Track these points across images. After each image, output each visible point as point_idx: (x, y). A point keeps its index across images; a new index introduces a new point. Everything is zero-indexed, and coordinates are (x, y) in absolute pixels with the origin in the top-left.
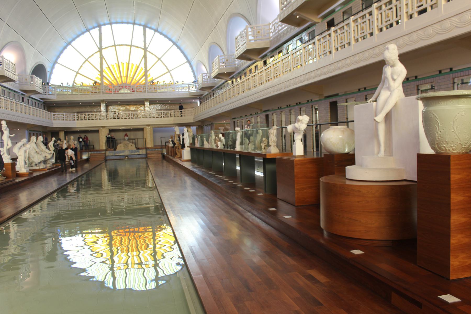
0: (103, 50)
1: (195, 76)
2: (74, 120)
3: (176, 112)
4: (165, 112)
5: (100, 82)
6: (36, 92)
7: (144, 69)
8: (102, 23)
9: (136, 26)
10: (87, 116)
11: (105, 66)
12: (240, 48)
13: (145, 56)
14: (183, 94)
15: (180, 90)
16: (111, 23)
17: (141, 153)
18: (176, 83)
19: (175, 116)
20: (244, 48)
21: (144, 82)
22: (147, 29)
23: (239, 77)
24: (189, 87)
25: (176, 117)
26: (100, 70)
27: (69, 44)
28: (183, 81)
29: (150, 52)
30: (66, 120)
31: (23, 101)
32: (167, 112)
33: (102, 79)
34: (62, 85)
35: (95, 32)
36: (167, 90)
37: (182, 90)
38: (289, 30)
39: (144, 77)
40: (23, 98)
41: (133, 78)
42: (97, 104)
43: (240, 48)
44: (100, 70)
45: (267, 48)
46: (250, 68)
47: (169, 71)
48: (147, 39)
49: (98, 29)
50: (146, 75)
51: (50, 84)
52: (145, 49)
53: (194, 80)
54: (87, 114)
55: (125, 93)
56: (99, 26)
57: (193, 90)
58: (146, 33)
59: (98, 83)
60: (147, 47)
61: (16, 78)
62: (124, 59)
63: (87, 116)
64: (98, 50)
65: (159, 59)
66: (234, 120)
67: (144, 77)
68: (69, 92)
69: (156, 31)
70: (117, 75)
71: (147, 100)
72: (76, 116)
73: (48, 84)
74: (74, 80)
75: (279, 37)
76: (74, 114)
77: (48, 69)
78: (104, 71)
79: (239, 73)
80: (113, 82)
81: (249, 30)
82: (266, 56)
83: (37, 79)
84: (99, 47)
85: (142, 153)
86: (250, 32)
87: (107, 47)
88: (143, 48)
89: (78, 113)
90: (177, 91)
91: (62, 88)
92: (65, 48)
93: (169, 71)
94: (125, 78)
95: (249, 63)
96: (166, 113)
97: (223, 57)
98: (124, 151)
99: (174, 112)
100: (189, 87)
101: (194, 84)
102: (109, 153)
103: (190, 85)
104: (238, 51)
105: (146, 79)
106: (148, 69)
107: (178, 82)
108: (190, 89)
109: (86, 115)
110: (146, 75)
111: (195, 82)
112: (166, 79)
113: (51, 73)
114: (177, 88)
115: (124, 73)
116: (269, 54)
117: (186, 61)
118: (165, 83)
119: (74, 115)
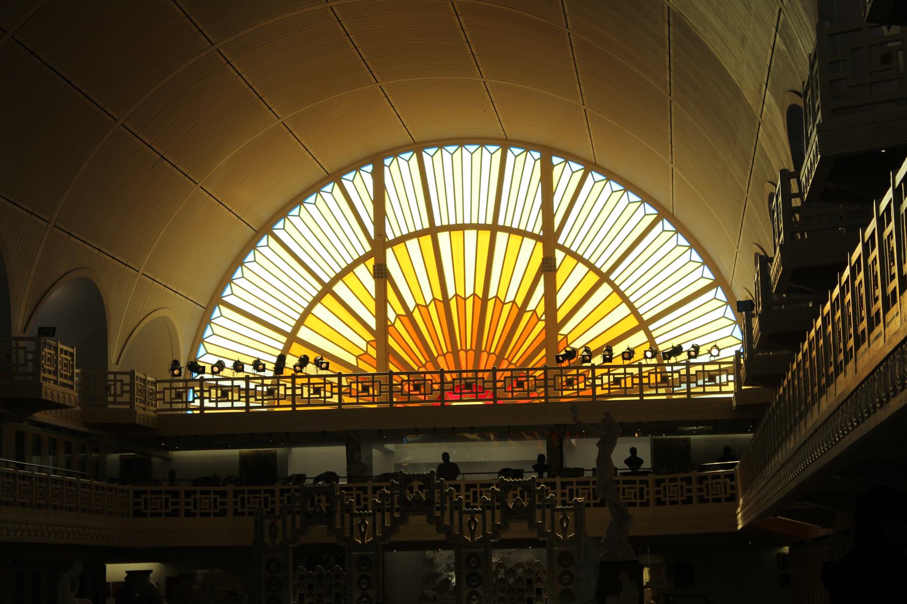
0: (389, 251)
7: (543, 318)
13: (548, 268)
16: (418, 148)
22: (556, 160)
26: (374, 327)
27: (266, 229)
29: (568, 252)
39: (543, 352)
44: (372, 322)
47: (643, 325)
49: (369, 168)
56: (377, 160)
64: (368, 248)
65: (604, 278)
67: (543, 352)
69: (590, 166)
78: (391, 329)
87: (402, 239)
93: (643, 325)
94: (471, 355)
106: (561, 315)
113: (198, 340)
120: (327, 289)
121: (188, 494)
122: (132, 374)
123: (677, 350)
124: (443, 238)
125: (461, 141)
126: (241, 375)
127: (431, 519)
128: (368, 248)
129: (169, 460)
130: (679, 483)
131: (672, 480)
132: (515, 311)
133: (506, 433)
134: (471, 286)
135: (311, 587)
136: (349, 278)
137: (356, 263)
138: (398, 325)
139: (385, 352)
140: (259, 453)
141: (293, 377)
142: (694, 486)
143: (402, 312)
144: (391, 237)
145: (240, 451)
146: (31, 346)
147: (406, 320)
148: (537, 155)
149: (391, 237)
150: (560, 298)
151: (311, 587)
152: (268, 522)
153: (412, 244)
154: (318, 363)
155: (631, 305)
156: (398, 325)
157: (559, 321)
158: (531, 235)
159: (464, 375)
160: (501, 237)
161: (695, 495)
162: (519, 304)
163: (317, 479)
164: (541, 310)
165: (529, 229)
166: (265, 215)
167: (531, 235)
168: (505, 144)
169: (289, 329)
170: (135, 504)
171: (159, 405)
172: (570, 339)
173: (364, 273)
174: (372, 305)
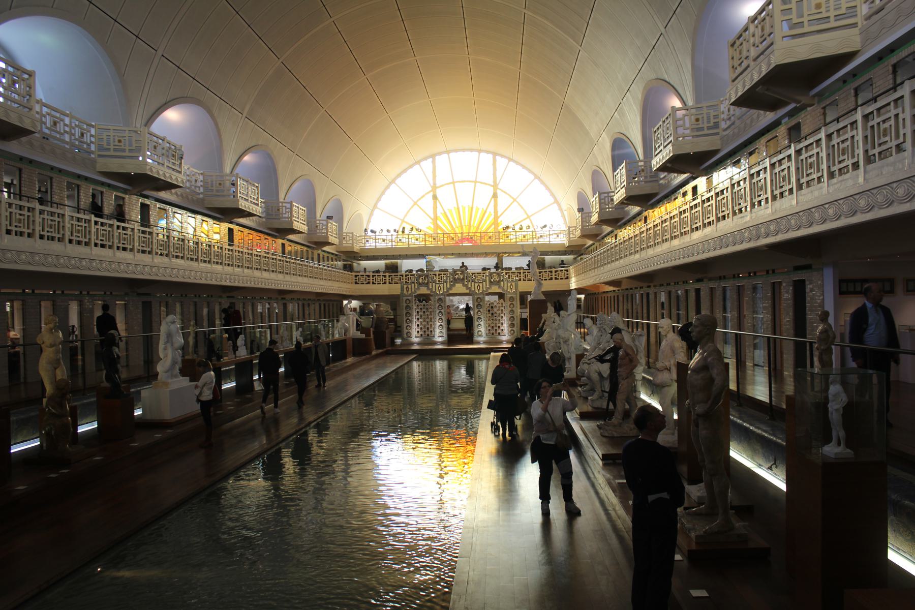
0: (437, 189)
7: (493, 214)
9: (482, 154)
11: (439, 210)
13: (495, 196)
16: (448, 152)
26: (433, 217)
27: (393, 181)
29: (502, 191)
35: (427, 164)
41: (478, 229)
44: (432, 216)
47: (528, 217)
50: (496, 223)
52: (495, 186)
56: (433, 156)
58: (497, 163)
64: (430, 189)
65: (515, 200)
67: (493, 226)
69: (510, 160)
84: (432, 185)
88: (492, 184)
92: (388, 187)
93: (528, 217)
94: (467, 227)
106: (499, 215)
110: (496, 223)
113: (369, 221)
115: (465, 222)
117: (552, 200)
121: (373, 276)
122: (352, 233)
123: (545, 226)
125: (464, 150)
126: (389, 234)
127: (464, 285)
128: (430, 189)
129: (359, 264)
130: (548, 273)
131: (545, 272)
133: (486, 254)
135: (421, 309)
137: (426, 194)
139: (437, 226)
140: (392, 263)
141: (408, 235)
142: (553, 274)
145: (386, 263)
146: (325, 223)
148: (491, 156)
151: (421, 309)
152: (405, 286)
154: (417, 230)
158: (489, 185)
159: (470, 234)
161: (553, 277)
163: (417, 271)
167: (489, 185)
168: (480, 151)
170: (356, 280)
171: (361, 245)
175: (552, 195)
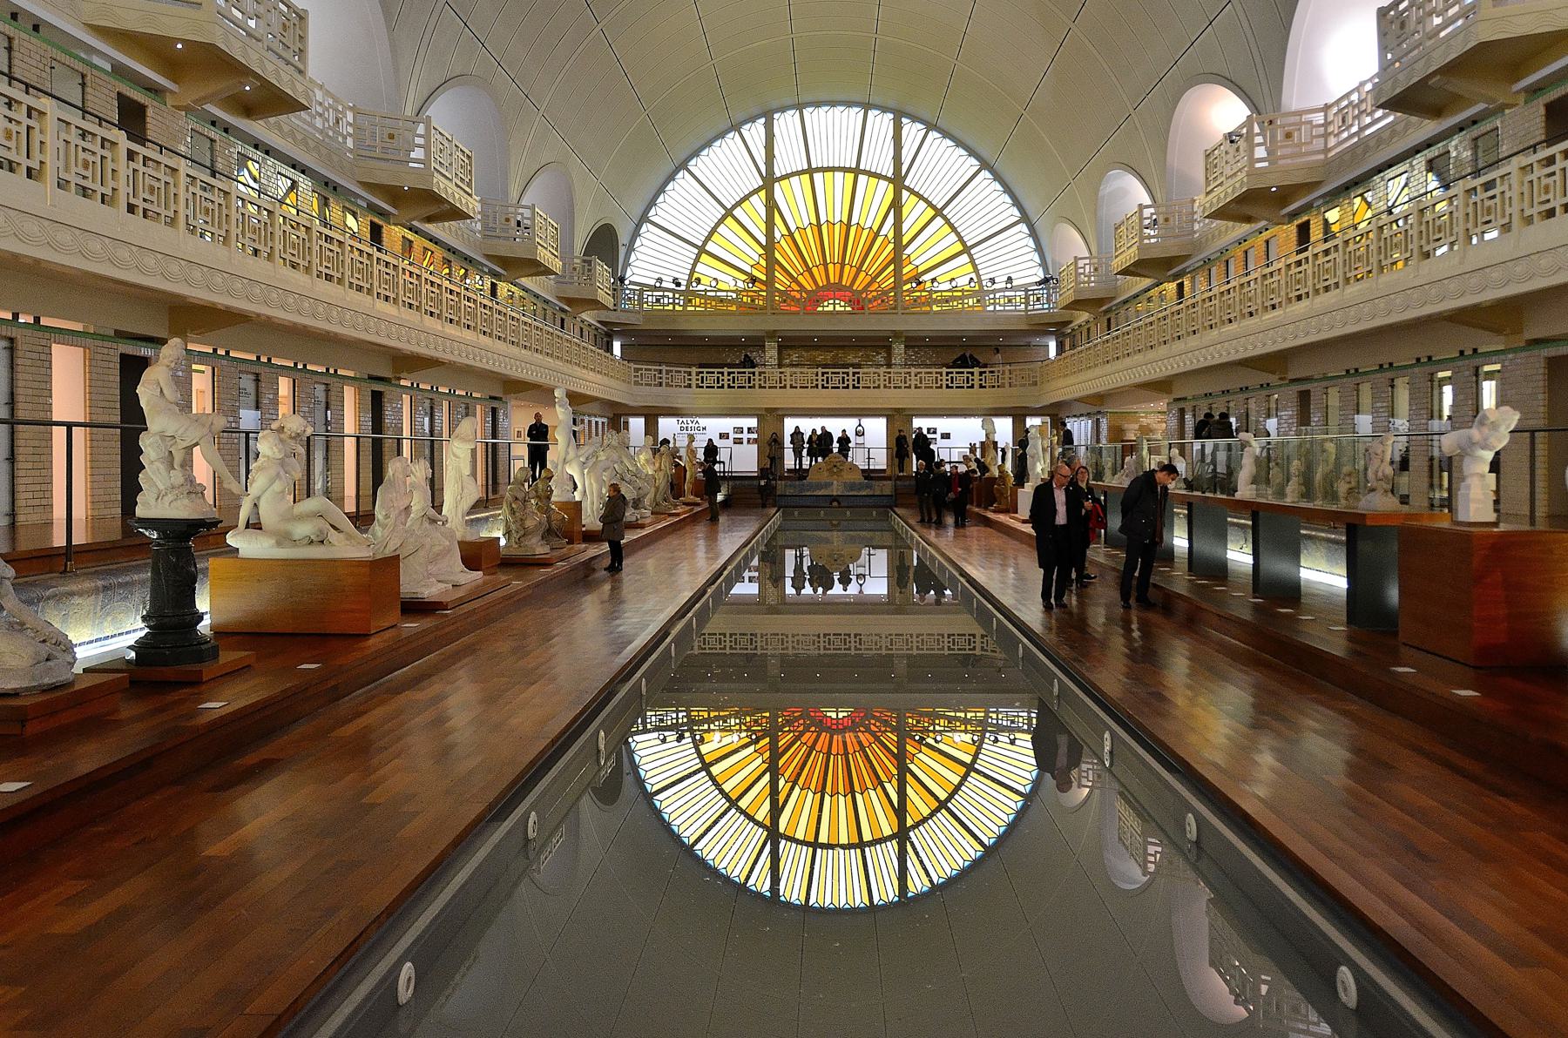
0: (776, 185)
1: (1044, 264)
2: (689, 386)
3: (987, 374)
4: (952, 373)
5: (764, 278)
6: (594, 304)
7: (893, 241)
8: (775, 105)
10: (726, 377)
12: (1221, 184)
13: (896, 205)
14: (1009, 318)
15: (998, 308)
16: (800, 107)
17: (878, 493)
18: (989, 284)
19: (981, 386)
20: (1237, 185)
21: (892, 279)
22: (904, 120)
23: (1207, 272)
24: (1027, 297)
25: (985, 387)
26: (764, 244)
27: (683, 166)
28: (1010, 280)
29: (912, 191)
30: (668, 385)
31: (562, 327)
32: (957, 373)
33: (769, 271)
34: (658, 285)
36: (960, 306)
37: (1007, 308)
38: (1399, 128)
39: (892, 267)
40: (563, 320)
41: (859, 270)
42: (757, 342)
43: (1221, 184)
44: (763, 240)
45: (1317, 184)
46: (1245, 246)
47: (967, 250)
48: (904, 152)
49: (763, 120)
50: (897, 259)
51: (627, 282)
52: (898, 180)
53: (1041, 275)
54: (726, 370)
55: (839, 313)
57: (1040, 306)
59: (761, 281)
60: (903, 175)
61: (556, 265)
62: (835, 211)
63: (726, 377)
64: (761, 183)
65: (939, 212)
66: (1182, 405)
67: (892, 267)
68: (678, 304)
69: (930, 126)
70: (813, 258)
71: (897, 335)
72: (694, 377)
73: (622, 280)
74: (693, 271)
75: (1359, 151)
76: (689, 370)
77: (623, 239)
79: (1208, 262)
80: (800, 278)
81: (1257, 129)
82: (1307, 208)
83: (602, 266)
84: (765, 175)
85: (882, 491)
86: (1258, 135)
89: (701, 366)
90: (991, 308)
91: (661, 293)
93: (967, 250)
95: (1243, 229)
96: (954, 375)
97: (1152, 210)
98: (828, 485)
99: (981, 373)
100: (1027, 297)
101: (1042, 289)
102: (786, 486)
103: (1031, 293)
104: (1214, 194)
105: (897, 273)
106: (905, 240)
107: (993, 281)
108: (1032, 303)
109: (722, 373)
111: (1045, 281)
112: (957, 274)
113: (631, 248)
114: (992, 301)
116: (1321, 201)
118: (954, 284)
119: (690, 374)
120: (729, 213)
124: (818, 177)
125: (833, 104)
128: (761, 183)
132: (872, 235)
134: (840, 214)
136: (746, 205)
138: (783, 242)
143: (786, 233)
144: (778, 174)
147: (789, 239)
148: (891, 116)
149: (778, 174)
150: (905, 227)
153: (794, 180)
155: (958, 234)
156: (783, 242)
157: (904, 244)
158: (885, 178)
160: (862, 178)
162: (875, 230)
164: (891, 235)
165: (884, 174)
166: (683, 157)
167: (885, 178)
168: (867, 107)
169: (700, 244)
172: (912, 258)
173: (758, 202)
174: (763, 227)
175: (1017, 203)
